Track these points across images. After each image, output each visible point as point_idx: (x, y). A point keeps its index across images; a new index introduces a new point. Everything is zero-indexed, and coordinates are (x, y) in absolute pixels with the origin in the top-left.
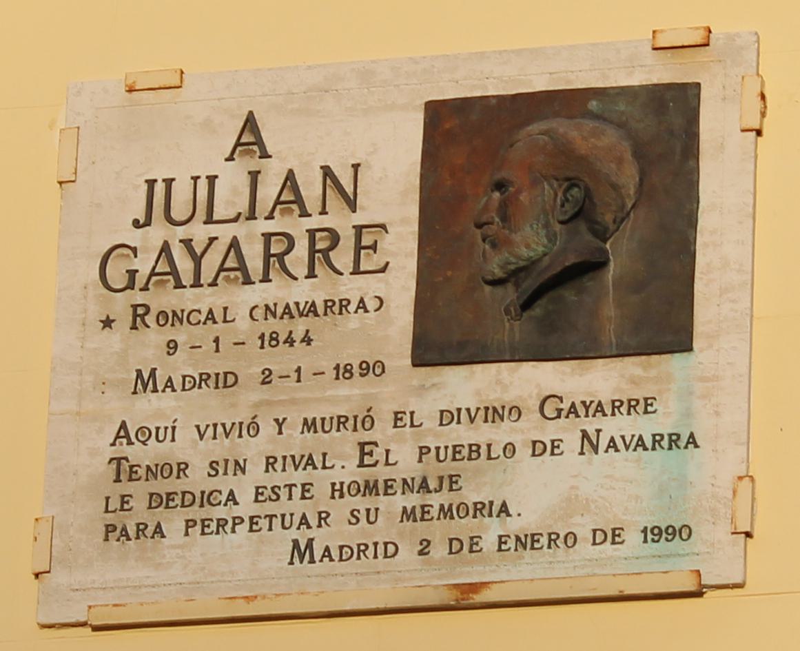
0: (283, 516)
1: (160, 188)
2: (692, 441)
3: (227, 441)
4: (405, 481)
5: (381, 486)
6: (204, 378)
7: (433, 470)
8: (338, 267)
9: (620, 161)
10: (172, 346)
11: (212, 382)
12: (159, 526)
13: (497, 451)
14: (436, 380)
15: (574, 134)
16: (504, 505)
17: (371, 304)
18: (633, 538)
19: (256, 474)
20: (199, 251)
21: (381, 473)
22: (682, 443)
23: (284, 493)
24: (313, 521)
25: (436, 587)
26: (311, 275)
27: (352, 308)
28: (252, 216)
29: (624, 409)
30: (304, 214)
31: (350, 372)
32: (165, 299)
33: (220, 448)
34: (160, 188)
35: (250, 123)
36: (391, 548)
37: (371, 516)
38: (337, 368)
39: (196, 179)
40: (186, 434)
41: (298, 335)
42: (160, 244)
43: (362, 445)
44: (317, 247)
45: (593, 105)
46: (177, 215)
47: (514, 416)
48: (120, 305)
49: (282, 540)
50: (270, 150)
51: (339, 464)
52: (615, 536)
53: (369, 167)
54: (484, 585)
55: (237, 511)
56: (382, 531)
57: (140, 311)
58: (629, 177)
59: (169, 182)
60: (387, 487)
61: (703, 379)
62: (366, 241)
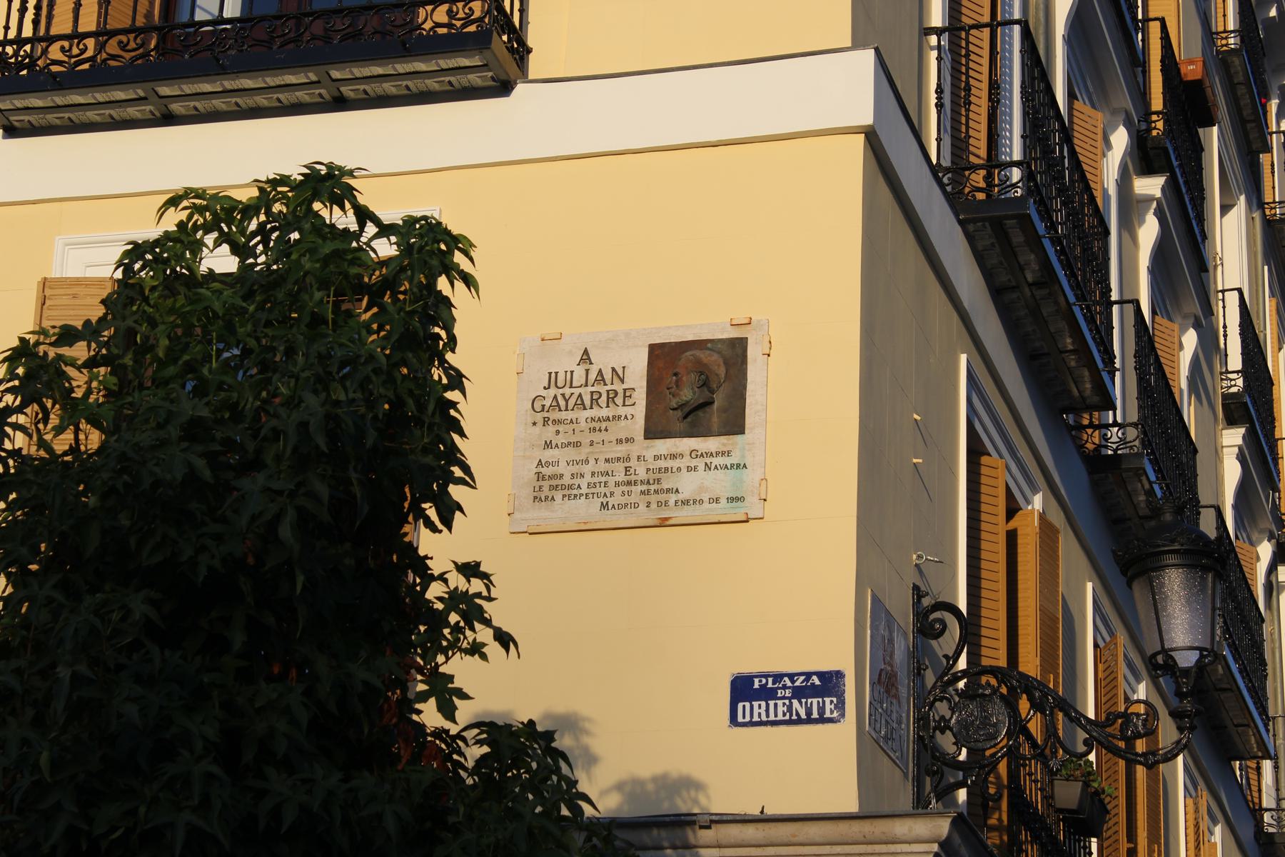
0: (598, 493)
1: (553, 375)
2: (745, 466)
3: (577, 467)
4: (641, 481)
5: (633, 482)
6: (569, 444)
7: (652, 476)
8: (617, 403)
9: (719, 365)
10: (558, 432)
11: (572, 445)
12: (553, 497)
13: (674, 470)
14: (653, 444)
15: (702, 356)
16: (677, 489)
17: (629, 417)
18: (723, 501)
19: (588, 478)
20: (567, 398)
21: (633, 478)
22: (741, 467)
23: (598, 485)
24: (608, 495)
25: (652, 519)
26: (608, 406)
27: (622, 418)
28: (586, 385)
29: (720, 455)
30: (605, 384)
31: (622, 441)
32: (555, 415)
33: (575, 469)
34: (553, 375)
35: (586, 352)
36: (636, 505)
37: (629, 493)
38: (617, 440)
39: (566, 372)
40: (563, 464)
41: (603, 428)
42: (553, 395)
43: (626, 468)
44: (610, 396)
45: (709, 345)
46: (559, 385)
47: (681, 457)
48: (539, 418)
49: (597, 502)
50: (593, 361)
51: (617, 474)
52: (717, 500)
53: (629, 368)
54: (670, 518)
55: (581, 492)
56: (633, 499)
57: (546, 419)
58: (722, 371)
59: (556, 373)
60: (635, 483)
61: (749, 444)
62: (628, 394)
